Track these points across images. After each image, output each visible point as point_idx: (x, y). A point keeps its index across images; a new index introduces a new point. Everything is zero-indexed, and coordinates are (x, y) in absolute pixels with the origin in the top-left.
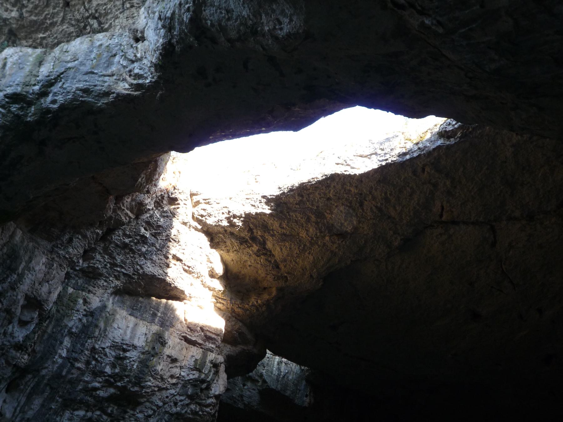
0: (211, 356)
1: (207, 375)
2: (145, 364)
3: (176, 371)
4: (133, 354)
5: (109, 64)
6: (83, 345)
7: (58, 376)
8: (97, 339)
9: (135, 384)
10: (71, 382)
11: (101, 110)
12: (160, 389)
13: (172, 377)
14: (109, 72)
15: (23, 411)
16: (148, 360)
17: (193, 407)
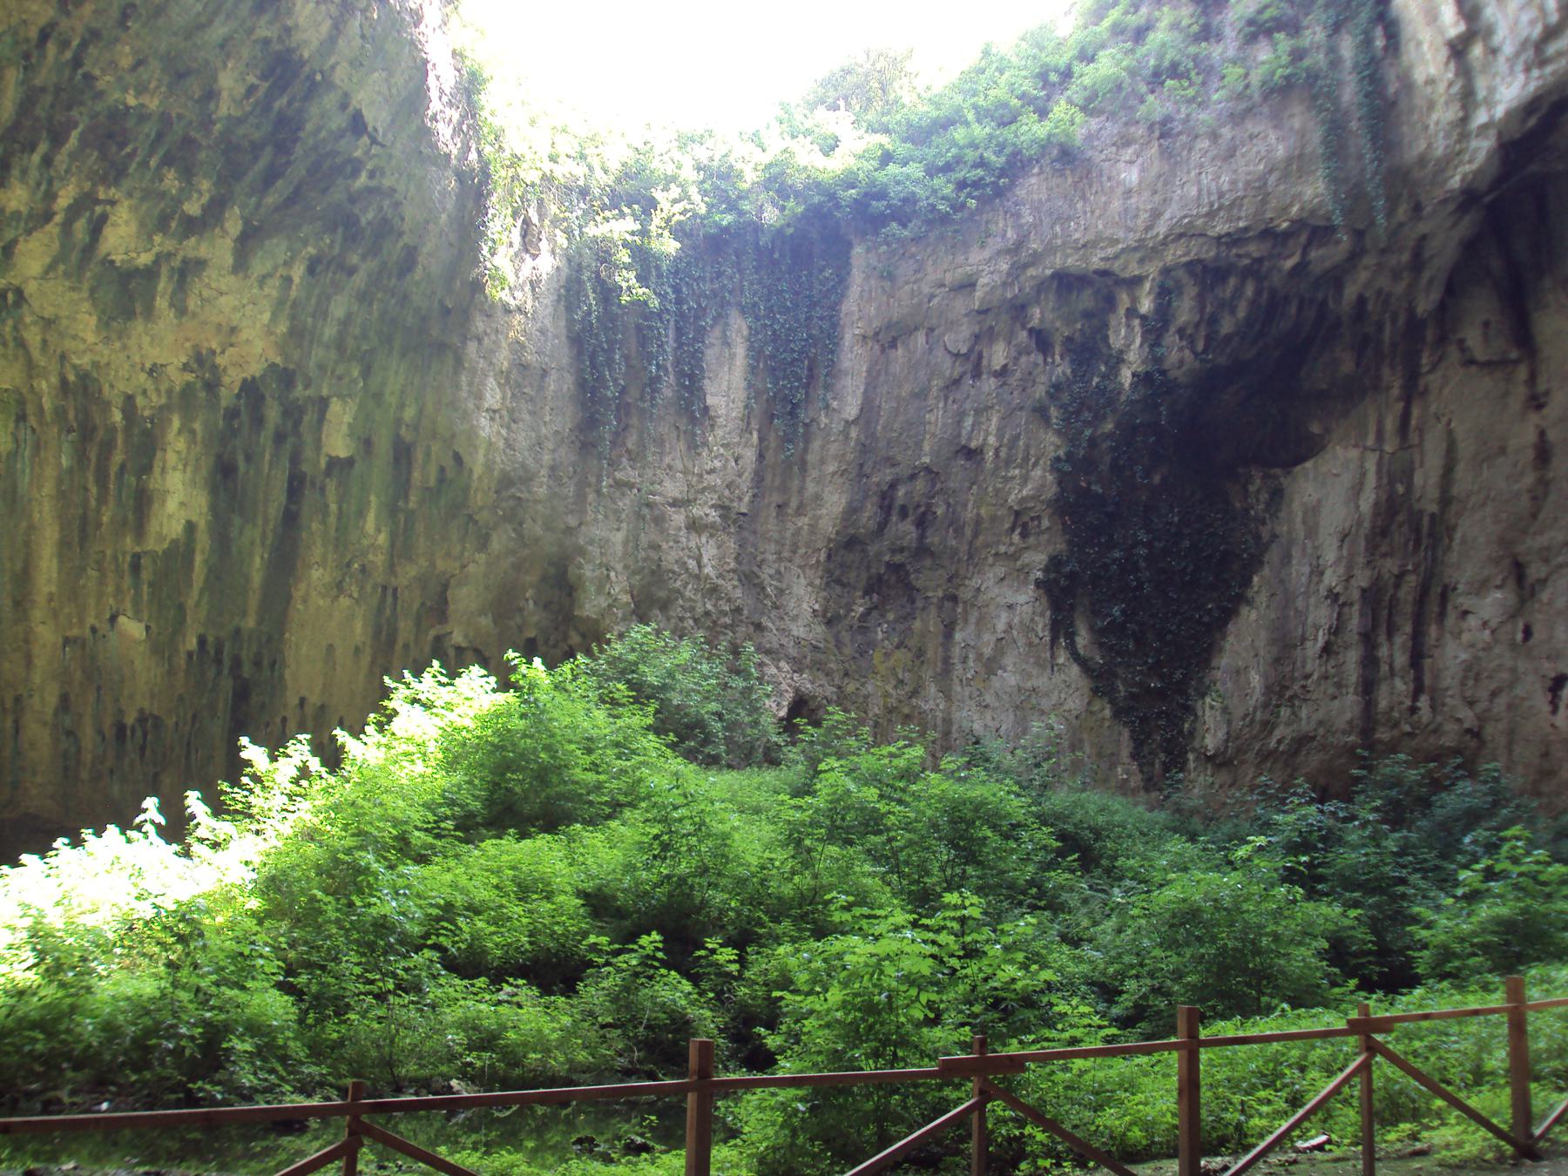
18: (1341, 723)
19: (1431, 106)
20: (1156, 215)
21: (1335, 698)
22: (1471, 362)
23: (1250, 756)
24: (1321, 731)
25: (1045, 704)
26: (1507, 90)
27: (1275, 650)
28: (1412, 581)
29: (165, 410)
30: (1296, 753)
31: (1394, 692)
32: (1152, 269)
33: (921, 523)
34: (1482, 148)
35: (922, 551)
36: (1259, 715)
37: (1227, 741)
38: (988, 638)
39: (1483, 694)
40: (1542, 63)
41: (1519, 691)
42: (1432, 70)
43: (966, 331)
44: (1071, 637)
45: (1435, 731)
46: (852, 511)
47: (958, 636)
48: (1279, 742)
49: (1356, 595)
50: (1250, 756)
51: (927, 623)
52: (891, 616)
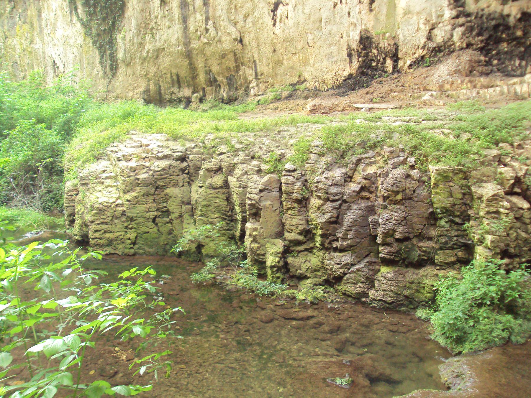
18: (173, 41)
21: (170, 27)
23: (137, 60)
24: (166, 46)
25: (72, 41)
27: (141, 5)
30: (157, 57)
31: (196, 20)
36: (135, 40)
37: (125, 53)
38: (52, 15)
39: (240, 17)
41: (257, 14)
44: (76, 9)
45: (219, 41)
47: (43, 15)
48: (148, 52)
50: (137, 60)
52: (20, 11)
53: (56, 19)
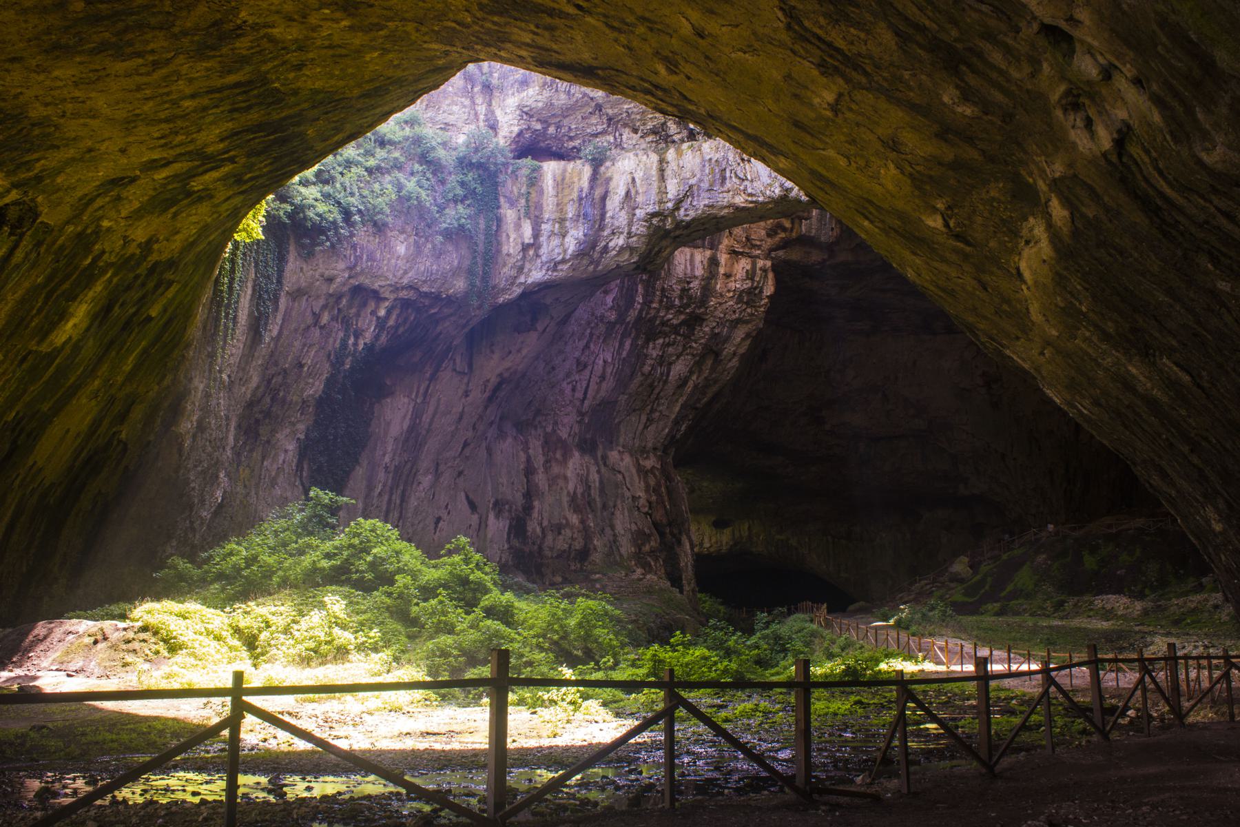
0: (760, 263)
1: (759, 282)
2: (707, 290)
3: (732, 285)
4: (695, 284)
5: (724, 179)
6: (654, 288)
7: (639, 318)
8: (664, 280)
9: (700, 308)
10: (649, 320)
11: (723, 217)
12: (721, 304)
13: (729, 291)
14: (725, 189)
15: (619, 353)
16: (709, 283)
17: (749, 310)
19: (505, 265)
20: (406, 272)
22: (455, 370)
26: (537, 275)
28: (409, 465)
29: (112, 265)
32: (392, 297)
33: (272, 399)
34: (517, 291)
35: (268, 414)
38: (275, 466)
40: (555, 269)
42: (511, 251)
43: (322, 302)
46: (258, 388)
49: (393, 468)
51: (257, 455)
53: (277, 474)
